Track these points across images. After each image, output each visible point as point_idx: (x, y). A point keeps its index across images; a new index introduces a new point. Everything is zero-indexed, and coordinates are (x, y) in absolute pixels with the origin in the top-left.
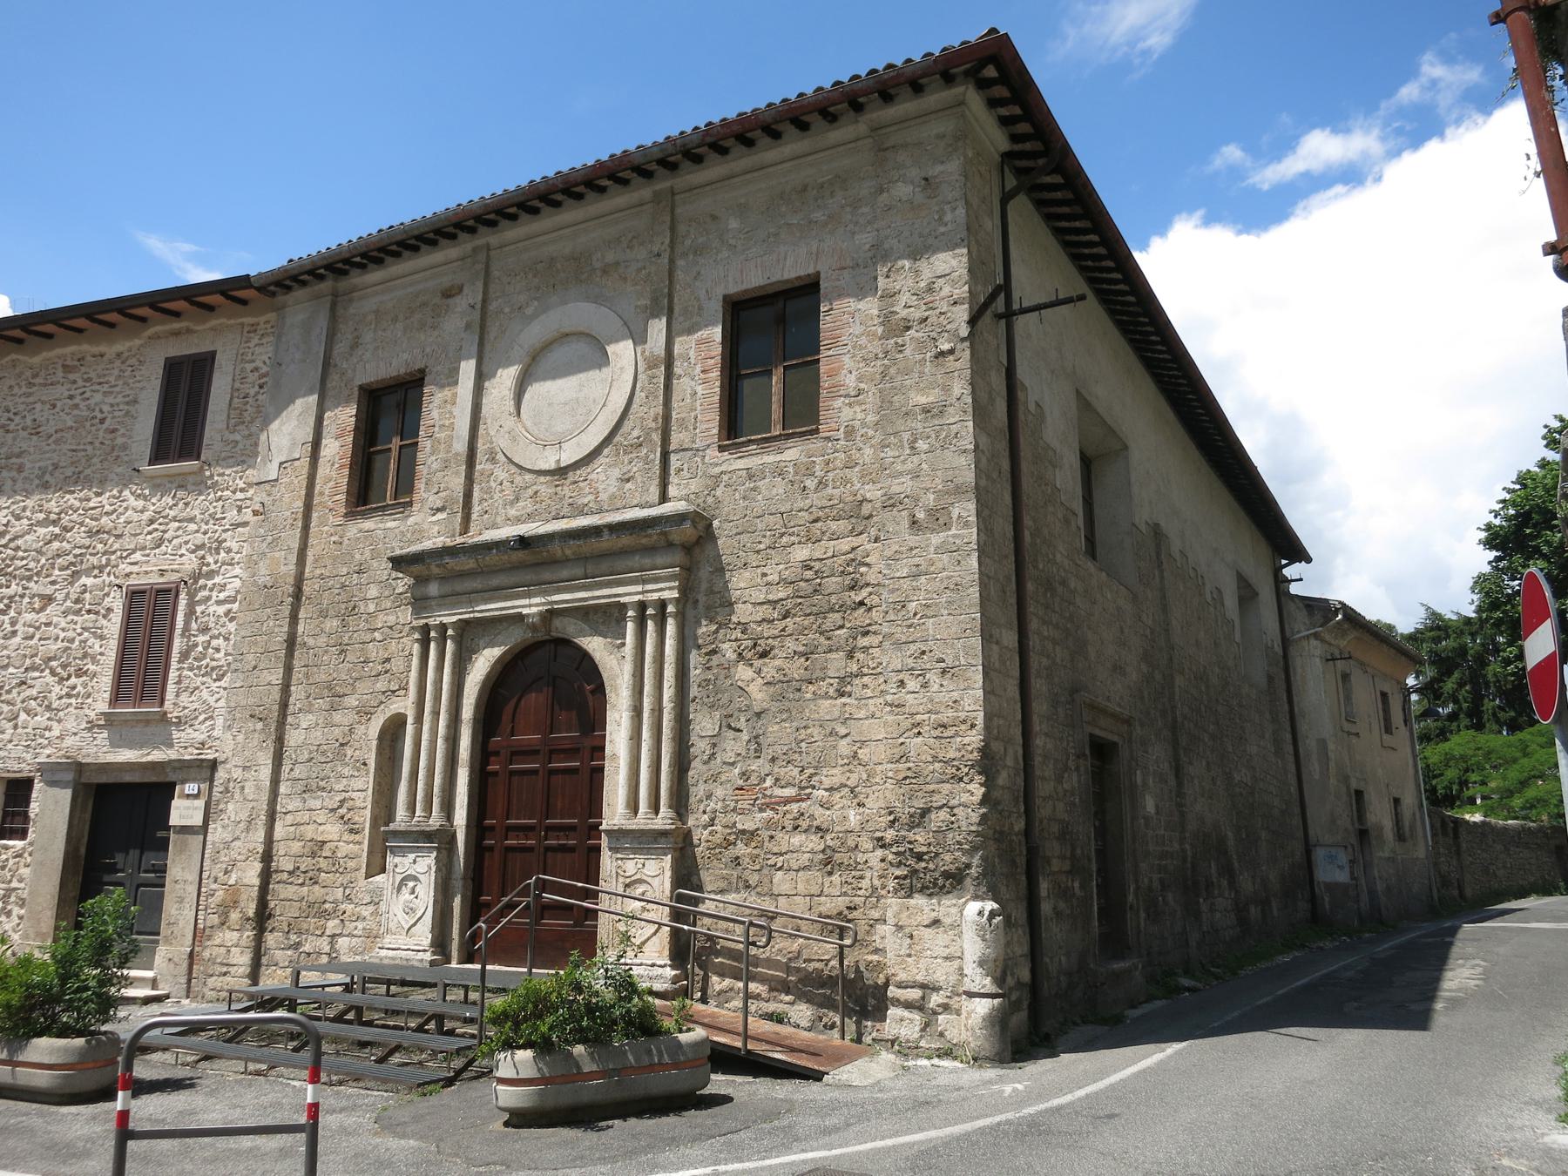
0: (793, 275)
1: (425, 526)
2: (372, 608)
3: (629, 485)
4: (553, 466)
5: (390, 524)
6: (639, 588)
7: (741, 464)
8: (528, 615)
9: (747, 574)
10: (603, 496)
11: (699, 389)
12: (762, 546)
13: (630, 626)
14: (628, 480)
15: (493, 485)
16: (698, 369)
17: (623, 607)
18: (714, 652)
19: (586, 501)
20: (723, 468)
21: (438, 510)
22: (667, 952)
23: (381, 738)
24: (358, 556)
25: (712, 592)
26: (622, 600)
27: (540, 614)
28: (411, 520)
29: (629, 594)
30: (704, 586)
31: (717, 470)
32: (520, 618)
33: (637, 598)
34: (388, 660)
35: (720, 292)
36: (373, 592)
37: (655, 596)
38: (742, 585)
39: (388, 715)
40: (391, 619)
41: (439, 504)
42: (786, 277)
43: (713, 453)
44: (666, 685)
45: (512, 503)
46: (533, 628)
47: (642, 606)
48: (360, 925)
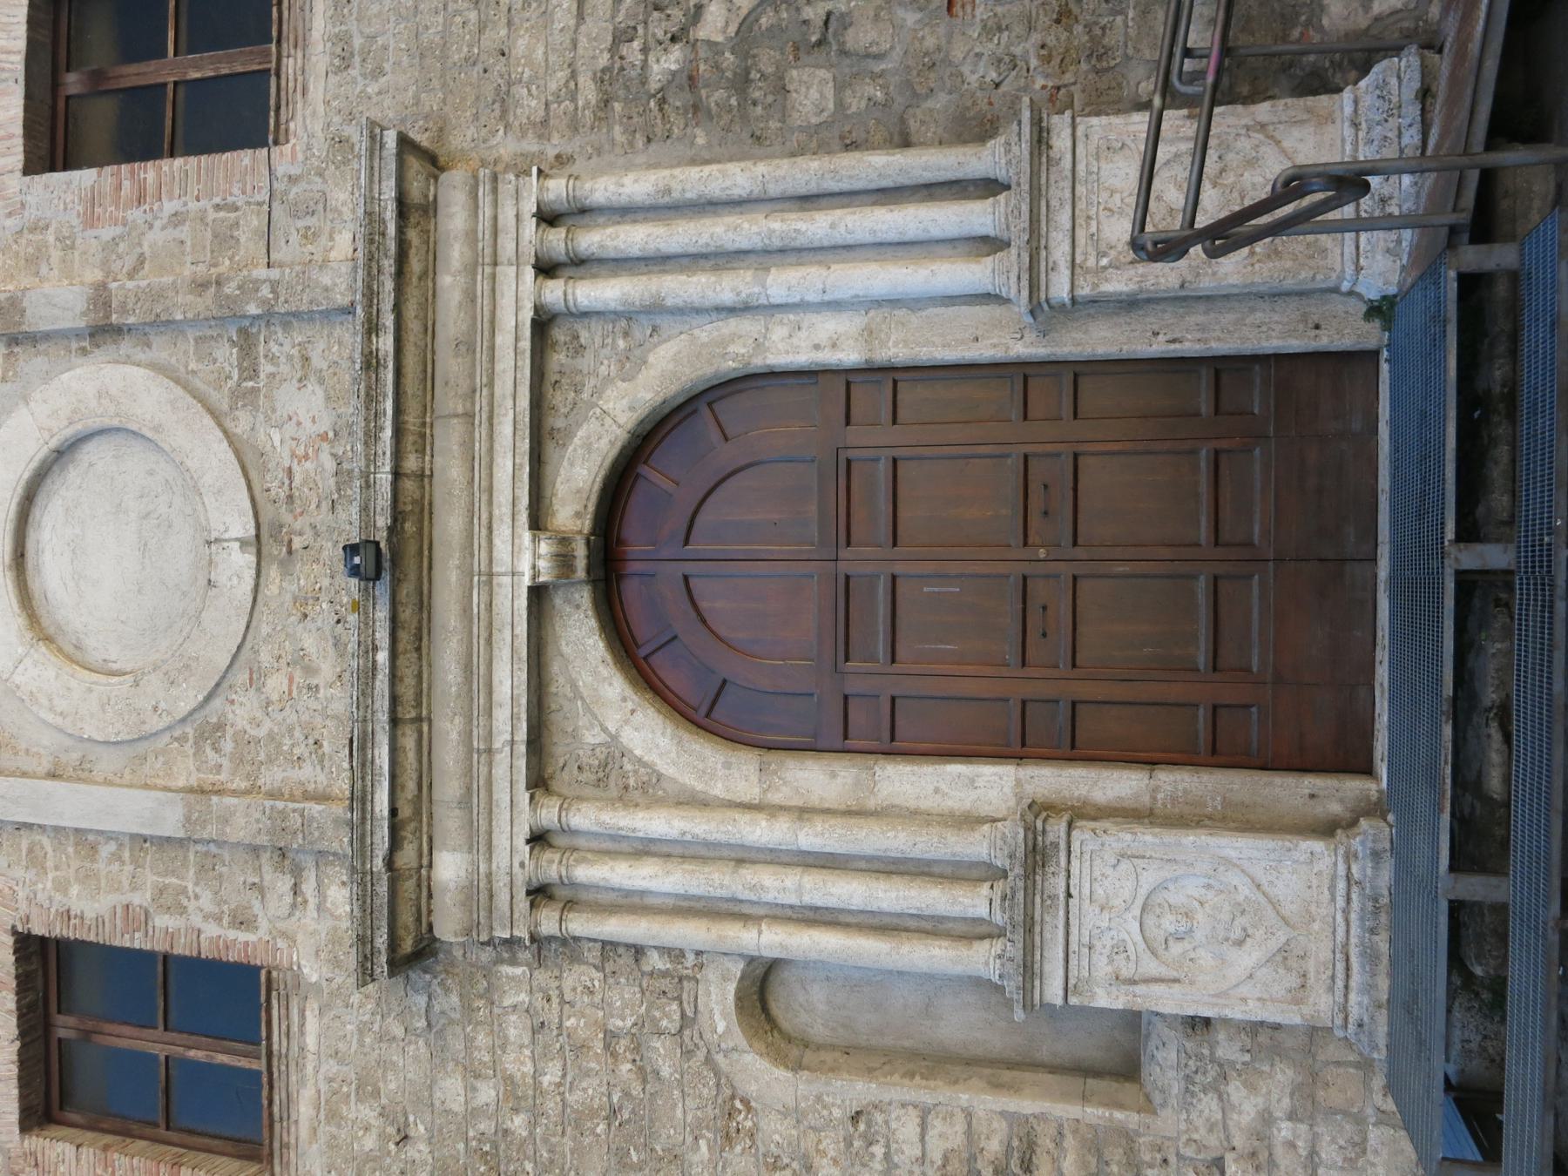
0: (21, 30)
1: (324, 926)
2: (487, 1093)
3: (317, 362)
4: (251, 558)
5: (311, 1041)
6: (507, 273)
7: (317, 91)
8: (536, 573)
9: (521, 45)
10: (325, 425)
11: (170, 206)
12: (473, 16)
13: (591, 293)
14: (306, 359)
15: (267, 725)
16: (136, 215)
17: (543, 324)
18: (662, 102)
19: (330, 465)
20: (317, 127)
21: (296, 890)
22: (1324, 100)
23: (797, 1067)
24: (370, 1142)
25: (545, 122)
26: (527, 315)
27: (535, 540)
28: (312, 972)
29: (518, 296)
30: (531, 145)
31: (320, 148)
32: (538, 594)
33: (529, 273)
34: (610, 1037)
35: (16, 182)
36: (451, 1089)
37: (530, 225)
38: (540, 52)
39: (738, 1038)
40: (516, 1029)
41: (284, 884)
42: (21, 44)
43: (286, 159)
44: (715, 189)
45: (310, 670)
46: (564, 561)
47: (546, 269)
48: (1284, 1130)
